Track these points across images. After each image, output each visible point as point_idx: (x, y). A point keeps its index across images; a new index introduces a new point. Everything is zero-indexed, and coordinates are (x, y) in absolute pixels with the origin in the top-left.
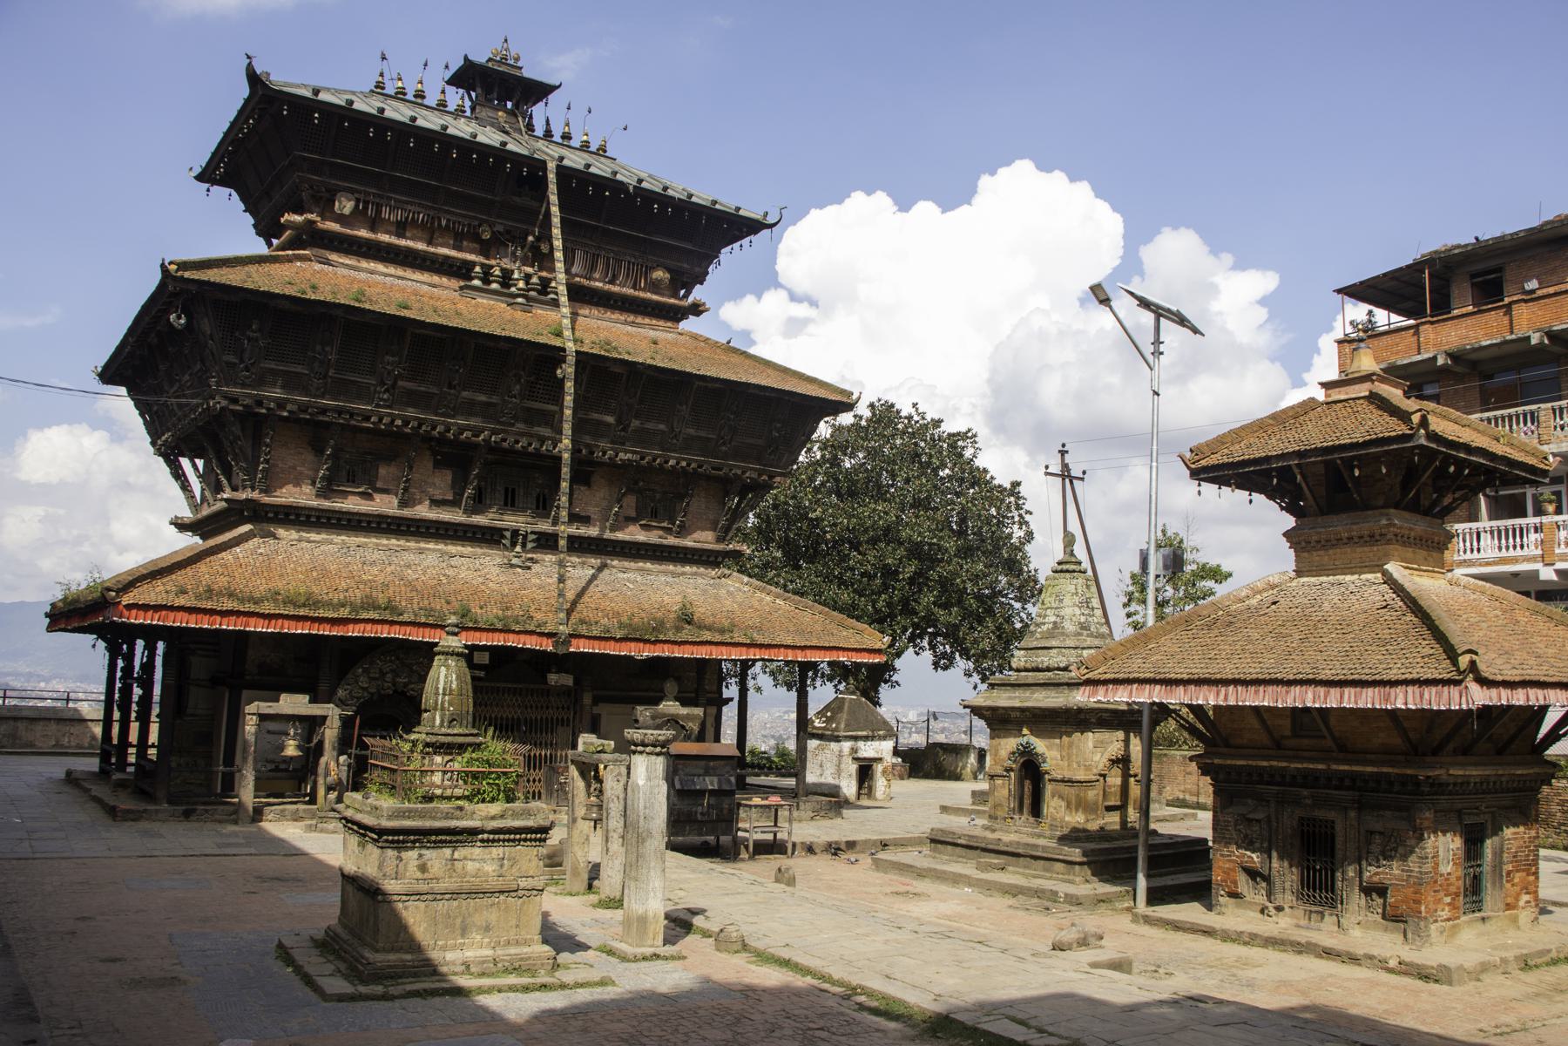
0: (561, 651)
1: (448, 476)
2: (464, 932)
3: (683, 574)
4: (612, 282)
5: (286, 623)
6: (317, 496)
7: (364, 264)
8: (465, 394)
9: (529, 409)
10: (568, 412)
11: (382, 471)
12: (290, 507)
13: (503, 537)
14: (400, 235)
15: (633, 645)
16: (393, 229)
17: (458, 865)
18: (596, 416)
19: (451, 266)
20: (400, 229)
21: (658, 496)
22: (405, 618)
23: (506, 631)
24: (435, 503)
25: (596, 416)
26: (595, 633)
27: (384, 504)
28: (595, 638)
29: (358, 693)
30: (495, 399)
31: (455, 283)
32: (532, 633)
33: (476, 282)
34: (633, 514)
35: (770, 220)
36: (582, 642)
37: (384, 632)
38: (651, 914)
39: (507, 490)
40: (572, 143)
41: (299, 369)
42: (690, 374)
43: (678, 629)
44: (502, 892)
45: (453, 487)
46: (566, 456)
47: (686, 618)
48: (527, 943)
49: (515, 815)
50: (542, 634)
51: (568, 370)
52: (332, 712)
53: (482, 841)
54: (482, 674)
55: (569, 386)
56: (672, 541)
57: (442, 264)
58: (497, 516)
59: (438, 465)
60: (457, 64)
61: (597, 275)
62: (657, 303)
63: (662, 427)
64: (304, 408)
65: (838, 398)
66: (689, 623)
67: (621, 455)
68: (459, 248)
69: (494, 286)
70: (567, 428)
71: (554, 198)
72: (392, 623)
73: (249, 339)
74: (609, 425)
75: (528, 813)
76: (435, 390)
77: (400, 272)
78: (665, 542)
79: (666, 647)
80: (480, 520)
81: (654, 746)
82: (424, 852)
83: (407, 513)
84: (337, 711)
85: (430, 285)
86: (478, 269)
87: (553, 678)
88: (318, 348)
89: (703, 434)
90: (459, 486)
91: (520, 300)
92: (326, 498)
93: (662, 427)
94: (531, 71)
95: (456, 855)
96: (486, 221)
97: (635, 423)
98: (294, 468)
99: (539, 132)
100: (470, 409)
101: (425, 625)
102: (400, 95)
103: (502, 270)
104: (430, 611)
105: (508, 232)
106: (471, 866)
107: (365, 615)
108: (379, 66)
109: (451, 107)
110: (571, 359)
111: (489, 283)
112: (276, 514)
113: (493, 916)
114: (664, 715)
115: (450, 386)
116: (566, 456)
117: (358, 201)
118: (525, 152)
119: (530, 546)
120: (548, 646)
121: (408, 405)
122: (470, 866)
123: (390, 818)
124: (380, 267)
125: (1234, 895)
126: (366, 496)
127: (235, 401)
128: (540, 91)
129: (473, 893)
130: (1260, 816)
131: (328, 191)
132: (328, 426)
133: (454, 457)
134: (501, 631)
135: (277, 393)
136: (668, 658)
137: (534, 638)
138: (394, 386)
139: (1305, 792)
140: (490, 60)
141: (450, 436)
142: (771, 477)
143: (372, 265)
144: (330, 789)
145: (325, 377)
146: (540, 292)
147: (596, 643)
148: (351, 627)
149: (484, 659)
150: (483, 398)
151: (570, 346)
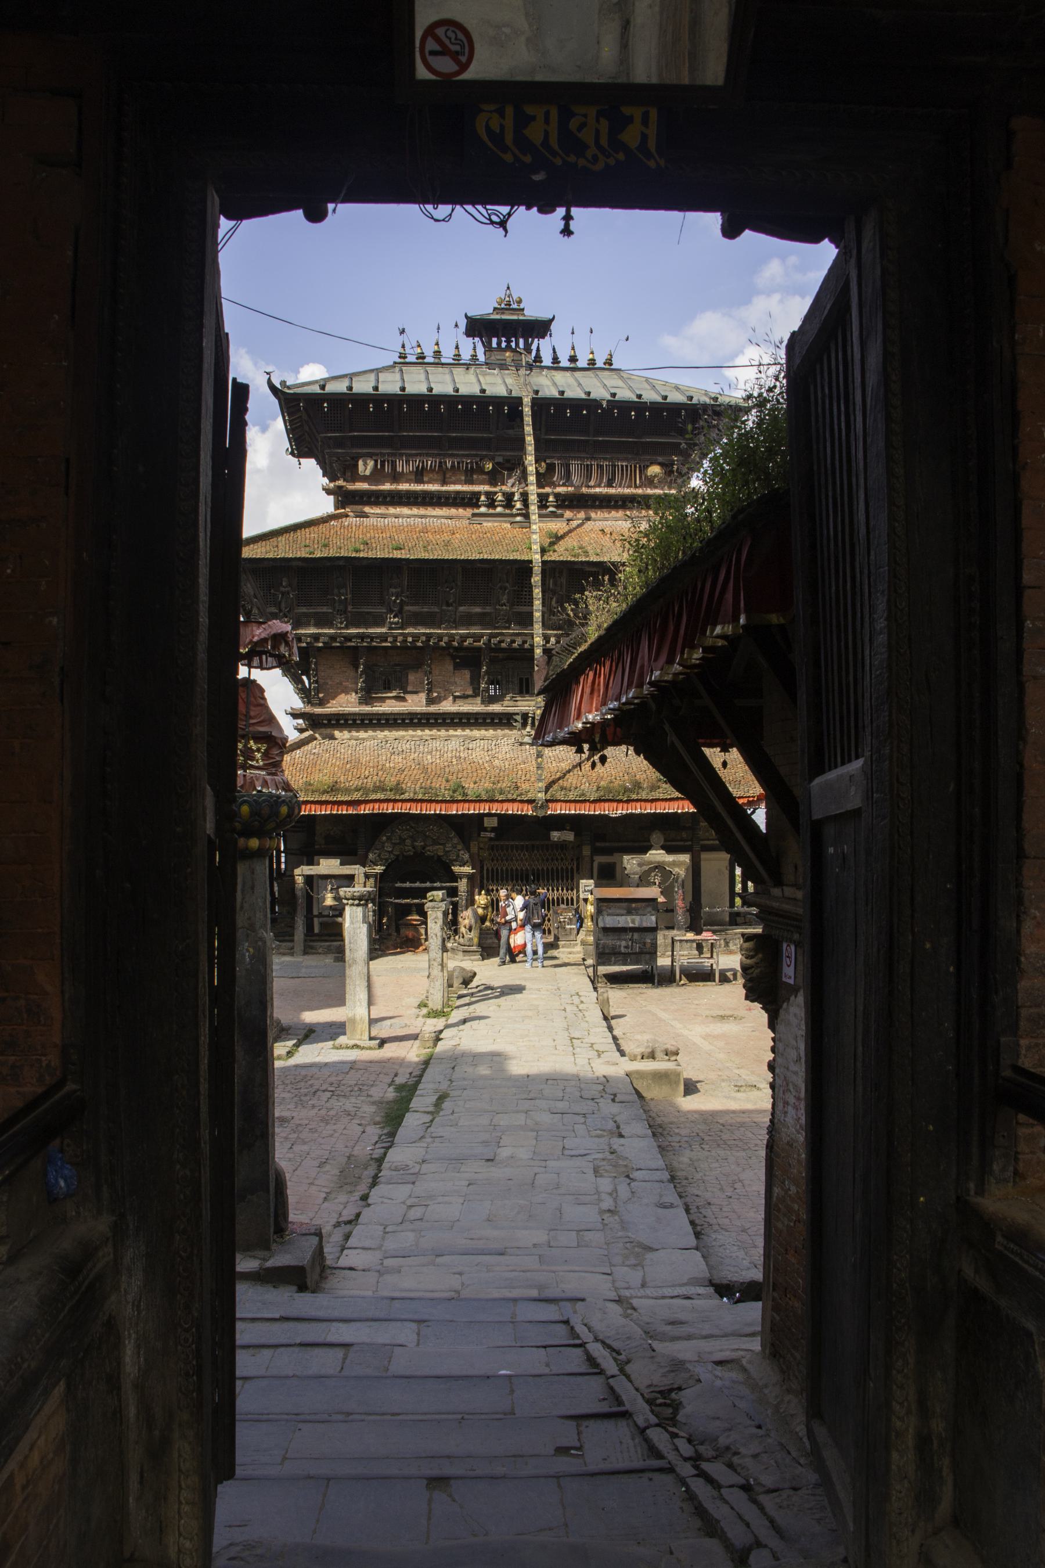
0: (541, 813)
1: (467, 674)
4: (610, 484)
5: (313, 807)
6: (360, 703)
7: (392, 510)
8: (462, 609)
9: (520, 613)
10: (537, 615)
11: (412, 677)
14: (422, 482)
15: (607, 805)
16: (413, 477)
20: (419, 476)
22: (406, 796)
23: (492, 801)
26: (571, 797)
27: (416, 703)
28: (570, 801)
30: (488, 609)
32: (514, 801)
33: (483, 510)
36: (559, 805)
37: (389, 809)
38: (358, 1017)
39: (521, 680)
40: (579, 364)
41: (325, 609)
45: (472, 683)
50: (522, 801)
51: (536, 579)
52: (357, 870)
54: (493, 835)
55: (537, 592)
57: (455, 499)
58: (511, 703)
59: (457, 667)
60: (463, 324)
61: (592, 483)
64: (333, 638)
69: (499, 509)
71: (528, 429)
72: (395, 801)
73: (283, 594)
76: (437, 610)
77: (422, 511)
79: (638, 805)
80: (496, 708)
83: (433, 709)
85: (447, 518)
86: (483, 498)
87: (555, 835)
88: (336, 591)
90: (475, 682)
91: (518, 519)
92: (367, 704)
94: (532, 311)
99: (547, 361)
100: (468, 620)
101: (422, 801)
103: (504, 494)
104: (426, 790)
105: (508, 461)
107: (373, 797)
108: (400, 339)
110: (537, 569)
111: (495, 507)
112: (329, 720)
114: (651, 863)
115: (448, 605)
117: (376, 461)
118: (504, 393)
120: (528, 811)
124: (405, 511)
126: (397, 698)
131: (353, 458)
132: (356, 648)
133: (467, 659)
134: (486, 801)
136: (641, 815)
137: (516, 805)
140: (495, 309)
143: (398, 510)
145: (345, 612)
147: (573, 805)
148: (363, 807)
149: (494, 823)
150: (478, 610)
151: (537, 558)
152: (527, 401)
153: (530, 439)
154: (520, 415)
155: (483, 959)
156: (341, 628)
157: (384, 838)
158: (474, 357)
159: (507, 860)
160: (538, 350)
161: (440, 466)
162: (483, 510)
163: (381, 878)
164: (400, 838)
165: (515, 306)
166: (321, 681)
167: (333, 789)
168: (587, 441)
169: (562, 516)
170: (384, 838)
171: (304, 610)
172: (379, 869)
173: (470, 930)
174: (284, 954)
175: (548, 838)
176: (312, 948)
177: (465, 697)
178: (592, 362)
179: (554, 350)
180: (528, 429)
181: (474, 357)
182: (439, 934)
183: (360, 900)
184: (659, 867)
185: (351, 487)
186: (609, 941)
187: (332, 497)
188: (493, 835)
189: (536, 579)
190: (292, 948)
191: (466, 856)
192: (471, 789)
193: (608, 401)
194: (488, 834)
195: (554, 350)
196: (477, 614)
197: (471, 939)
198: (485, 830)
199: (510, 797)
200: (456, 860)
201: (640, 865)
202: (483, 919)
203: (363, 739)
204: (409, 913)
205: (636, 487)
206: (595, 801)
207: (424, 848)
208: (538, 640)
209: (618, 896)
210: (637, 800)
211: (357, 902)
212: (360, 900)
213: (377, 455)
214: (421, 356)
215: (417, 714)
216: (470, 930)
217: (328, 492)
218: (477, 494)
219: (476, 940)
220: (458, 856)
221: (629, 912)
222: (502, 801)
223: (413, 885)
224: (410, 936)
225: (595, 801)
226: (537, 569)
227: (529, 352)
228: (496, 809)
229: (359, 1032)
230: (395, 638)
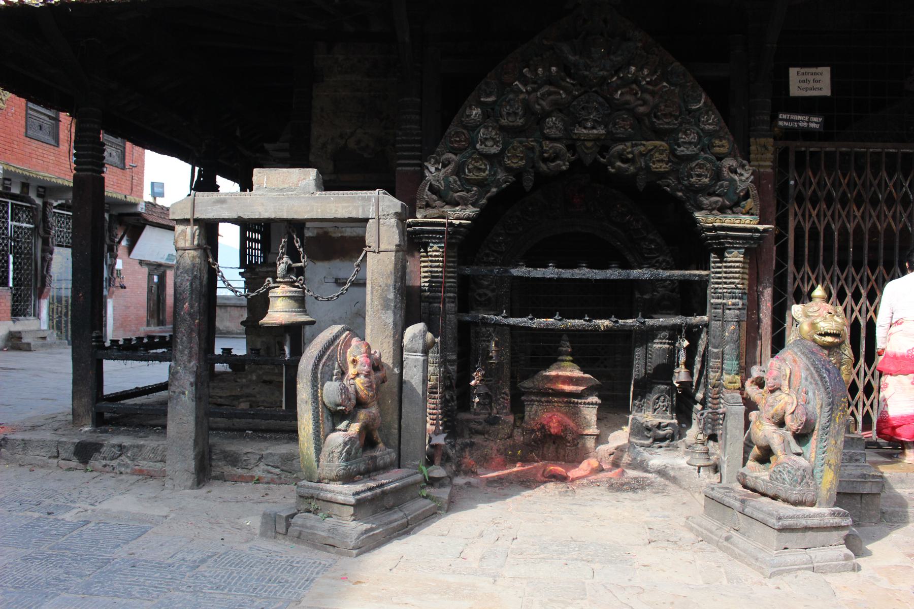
29: (480, 171)
54: (815, 123)
84: (390, 204)
144: (337, 416)
157: (476, 112)
159: (859, 203)
163: (465, 245)
164: (528, 109)
170: (476, 112)
172: (459, 215)
173: (802, 437)
176: (234, 460)
188: (815, 123)
191: (744, 178)
194: (802, 121)
197: (807, 476)
207: (604, 149)
220: (717, 176)
223: (567, 274)
224: (554, 428)
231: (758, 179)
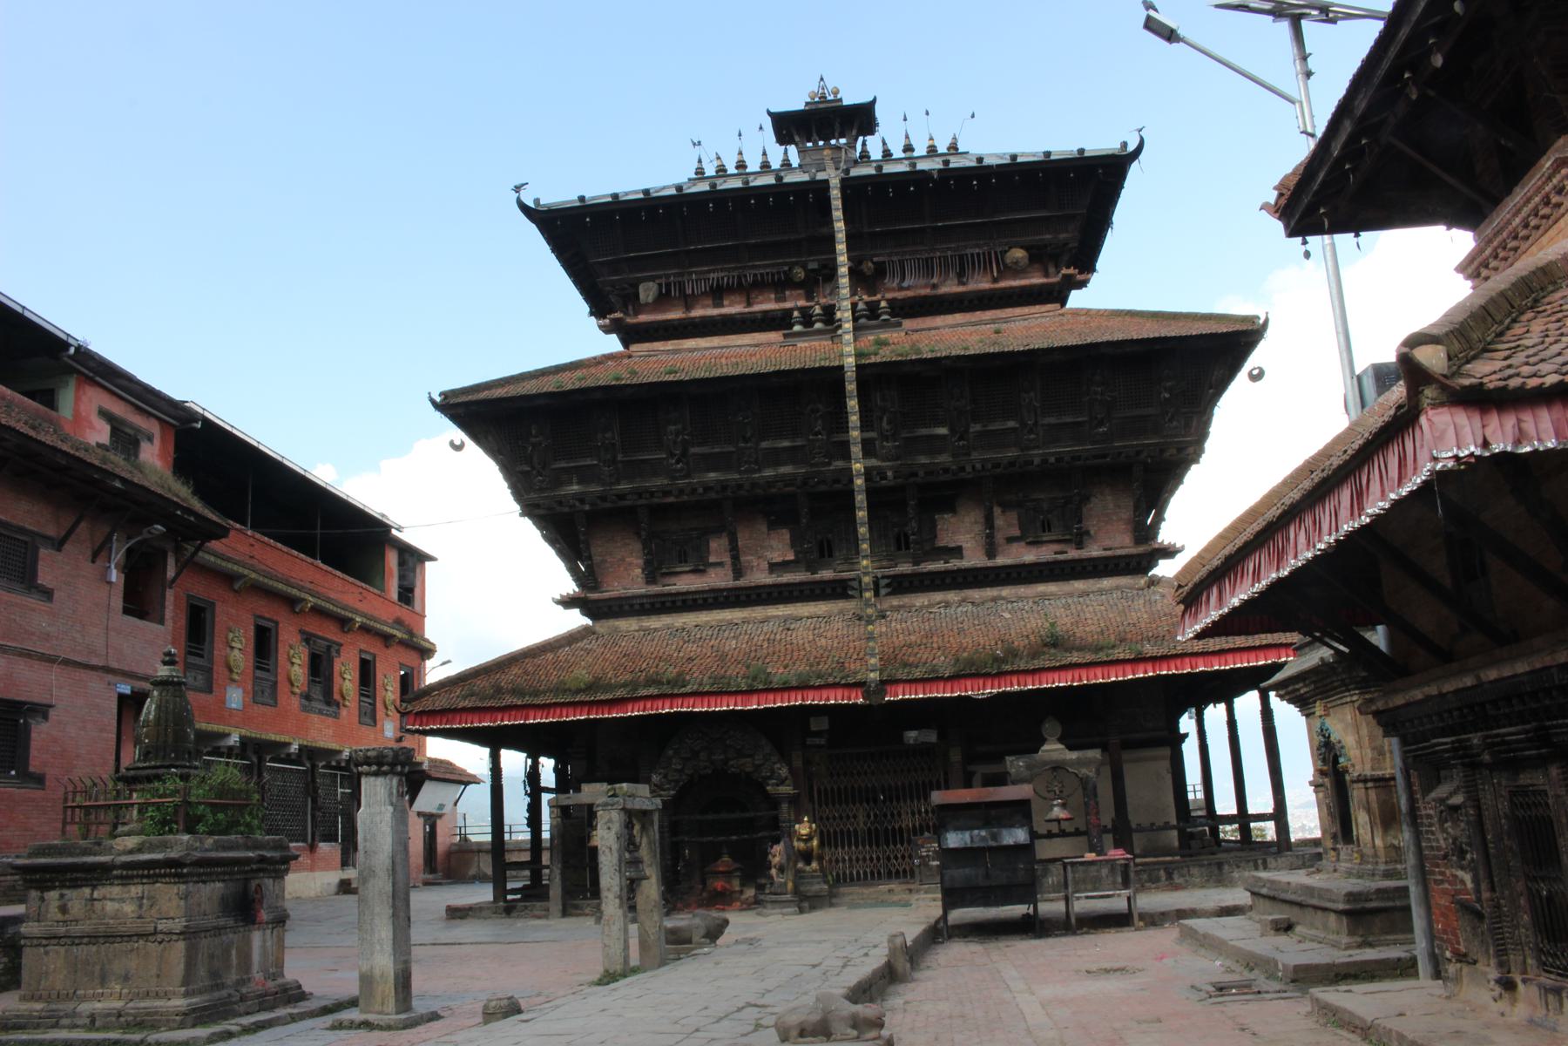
0: (875, 701)
1: (786, 535)
2: (103, 981)
3: (1101, 592)
4: (964, 284)
8: (764, 444)
11: (713, 545)
12: (619, 599)
13: (887, 586)
17: (98, 905)
18: (924, 431)
19: (773, 319)
21: (1045, 506)
22: (688, 689)
23: (803, 687)
24: (774, 567)
25: (924, 431)
26: (917, 674)
28: (916, 681)
31: (774, 336)
32: (835, 686)
33: (797, 328)
34: (1016, 532)
35: (1131, 148)
38: (377, 972)
40: (916, 154)
41: (589, 462)
42: (1012, 354)
43: (1034, 655)
44: (140, 936)
45: (793, 545)
46: (859, 482)
47: (1055, 642)
48: (167, 996)
49: (152, 848)
51: (851, 387)
53: (117, 877)
54: (823, 742)
55: (853, 404)
56: (1073, 554)
57: (763, 320)
58: (845, 567)
59: (773, 526)
61: (935, 280)
62: (1023, 288)
63: (1011, 424)
64: (603, 498)
65: (1238, 327)
66: (1055, 645)
67: (969, 469)
68: (784, 300)
69: (818, 325)
70: (856, 450)
71: (838, 214)
72: (673, 696)
74: (943, 437)
75: (164, 846)
78: (1061, 557)
80: (826, 574)
81: (369, 765)
82: (65, 891)
83: (741, 583)
86: (796, 314)
87: (911, 736)
89: (1068, 419)
93: (1011, 424)
95: (96, 895)
96: (796, 263)
97: (976, 428)
98: (623, 560)
100: (775, 458)
102: (721, 170)
104: (715, 679)
106: (110, 907)
109: (776, 164)
110: (850, 375)
111: (812, 325)
113: (132, 963)
114: (1045, 763)
115: (746, 440)
116: (859, 482)
119: (883, 592)
121: (709, 471)
122: (110, 907)
123: (30, 856)
125: (1461, 957)
127: (538, 506)
128: (861, 118)
129: (110, 937)
130: (1458, 799)
132: (632, 510)
135: (575, 488)
136: (1021, 693)
137: (839, 692)
138: (684, 453)
139: (1475, 739)
141: (759, 491)
142: (1180, 450)
146: (869, 318)
149: (819, 724)
150: (786, 444)
152: (835, 182)
153: (840, 226)
154: (828, 200)
155: (802, 911)
156: (612, 484)
157: (671, 752)
158: (786, 164)
160: (864, 144)
161: (740, 283)
162: (797, 328)
165: (831, 97)
166: (597, 559)
167: (591, 687)
168: (922, 230)
169: (900, 325)
170: (671, 752)
171: (563, 465)
174: (539, 917)
175: (901, 737)
176: (576, 907)
177: (783, 566)
178: (932, 151)
179: (884, 143)
180: (838, 214)
181: (786, 164)
182: (615, 847)
183: (380, 764)
184: (1058, 767)
185: (629, 320)
186: (959, 874)
187: (614, 336)
189: (851, 387)
190: (547, 910)
191: (784, 772)
192: (778, 673)
193: (940, 171)
194: (817, 741)
195: (884, 143)
196: (785, 449)
198: (818, 734)
199: (831, 680)
200: (770, 778)
201: (1028, 767)
202: (807, 856)
203: (656, 630)
204: (718, 856)
205: (995, 280)
206: (951, 678)
208: (857, 466)
209: (968, 800)
210: (1012, 673)
211: (374, 768)
212: (380, 764)
213: (660, 277)
214: (721, 170)
215: (721, 590)
216: (781, 869)
217: (607, 330)
218: (788, 313)
219: (790, 885)
220: (773, 772)
221: (986, 823)
222: (820, 687)
225: (951, 678)
226: (850, 375)
227: (854, 148)
228: (812, 699)
229: (379, 1000)
230: (681, 492)
231: (791, 770)
